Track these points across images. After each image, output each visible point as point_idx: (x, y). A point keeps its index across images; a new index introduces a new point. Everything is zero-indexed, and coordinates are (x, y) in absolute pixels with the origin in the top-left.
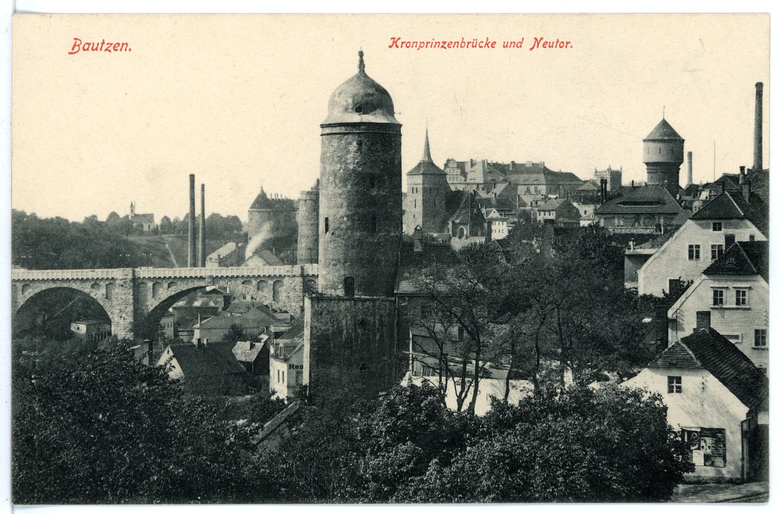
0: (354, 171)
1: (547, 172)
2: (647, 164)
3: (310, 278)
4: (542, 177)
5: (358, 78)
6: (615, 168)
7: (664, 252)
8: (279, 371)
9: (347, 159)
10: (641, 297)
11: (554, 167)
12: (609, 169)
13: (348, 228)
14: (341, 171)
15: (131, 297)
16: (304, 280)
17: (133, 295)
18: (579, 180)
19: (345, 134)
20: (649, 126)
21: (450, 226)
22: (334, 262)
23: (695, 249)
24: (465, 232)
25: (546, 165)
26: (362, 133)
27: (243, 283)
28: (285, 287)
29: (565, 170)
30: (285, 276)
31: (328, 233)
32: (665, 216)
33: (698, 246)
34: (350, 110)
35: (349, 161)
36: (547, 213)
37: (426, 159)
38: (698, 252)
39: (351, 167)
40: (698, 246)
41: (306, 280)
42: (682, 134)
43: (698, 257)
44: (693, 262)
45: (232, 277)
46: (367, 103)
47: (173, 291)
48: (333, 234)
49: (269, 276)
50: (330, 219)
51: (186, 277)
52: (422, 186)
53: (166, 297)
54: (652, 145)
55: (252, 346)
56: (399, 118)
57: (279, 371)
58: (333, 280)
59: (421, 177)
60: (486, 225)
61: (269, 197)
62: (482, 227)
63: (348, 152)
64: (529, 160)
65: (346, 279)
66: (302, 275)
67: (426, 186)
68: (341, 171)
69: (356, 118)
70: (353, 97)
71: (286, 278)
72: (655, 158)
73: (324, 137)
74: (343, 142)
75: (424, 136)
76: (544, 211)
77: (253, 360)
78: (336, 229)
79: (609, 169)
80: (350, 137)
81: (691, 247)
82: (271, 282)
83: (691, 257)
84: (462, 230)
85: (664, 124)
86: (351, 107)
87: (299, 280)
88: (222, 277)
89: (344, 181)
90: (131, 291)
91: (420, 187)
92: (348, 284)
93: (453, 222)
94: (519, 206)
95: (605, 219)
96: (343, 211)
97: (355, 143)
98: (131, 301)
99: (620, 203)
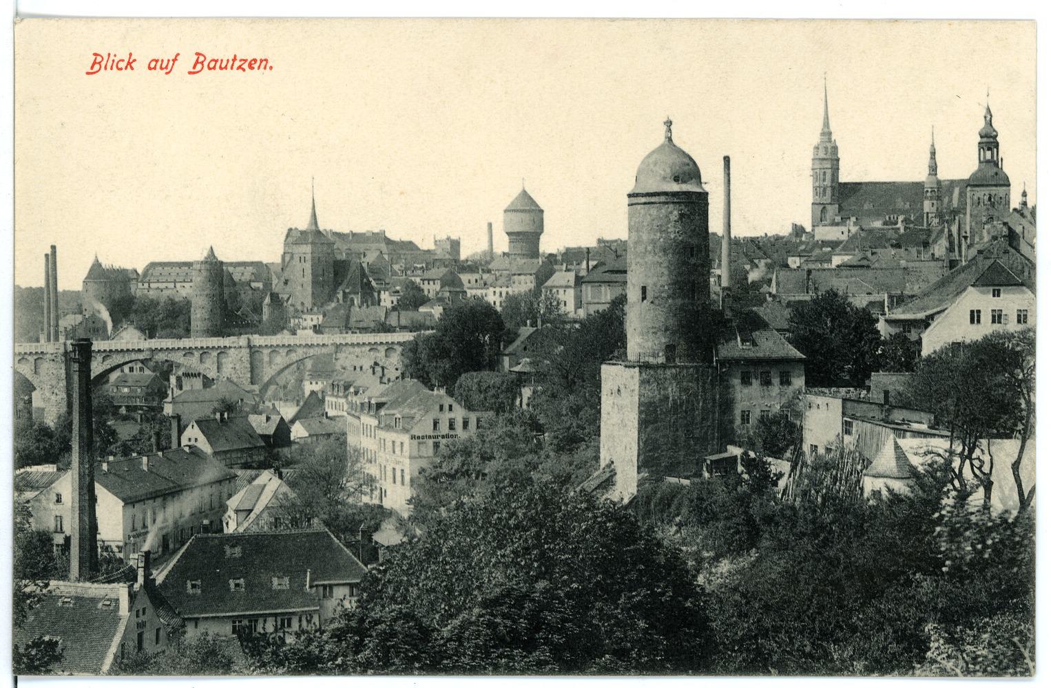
0: (675, 240)
1: (389, 242)
2: (508, 234)
3: (257, 349)
4: (383, 246)
5: (662, 146)
6: (454, 237)
7: (946, 316)
8: (393, 442)
9: (668, 228)
10: (925, 360)
11: (394, 235)
12: (448, 239)
13: (669, 297)
14: (662, 240)
15: (63, 371)
16: (250, 351)
17: (66, 369)
18: (418, 249)
19: (667, 203)
20: (509, 196)
21: (340, 296)
22: (654, 330)
23: (976, 314)
24: (355, 302)
25: (386, 235)
26: (683, 203)
27: (184, 355)
28: (230, 359)
29: (406, 238)
30: (230, 347)
31: (645, 301)
32: (593, 284)
33: (979, 311)
34: (668, 179)
35: (669, 230)
36: (431, 283)
37: (314, 228)
38: (979, 317)
39: (672, 236)
40: (979, 311)
41: (253, 350)
42: (542, 203)
43: (979, 321)
44: (975, 326)
45: (173, 349)
46: (684, 173)
47: (108, 365)
48: (652, 302)
49: (213, 347)
50: (649, 288)
51: (122, 351)
52: (310, 255)
53: (101, 371)
54: (511, 215)
55: (268, 419)
56: (706, 188)
57: (393, 442)
58: (652, 347)
59: (310, 246)
60: (376, 294)
61: (103, 266)
62: (372, 296)
63: (669, 222)
64: (370, 229)
65: (667, 347)
66: (250, 347)
67: (315, 255)
68: (662, 240)
69: (675, 187)
70: (671, 168)
71: (233, 350)
72: (517, 229)
73: (816, 206)
74: (663, 211)
75: (311, 206)
76: (429, 280)
77: (272, 433)
78: (657, 298)
79: (448, 239)
80: (671, 206)
81: (972, 312)
82: (215, 353)
83: (972, 321)
84: (352, 300)
85: (525, 194)
86: (669, 176)
87: (245, 352)
88: (162, 349)
89: (664, 250)
90: (63, 366)
91: (309, 257)
92: (670, 349)
93: (344, 292)
94: (392, 275)
95: (592, 287)
96: (665, 280)
97: (676, 212)
98: (64, 376)
99: (605, 272)
